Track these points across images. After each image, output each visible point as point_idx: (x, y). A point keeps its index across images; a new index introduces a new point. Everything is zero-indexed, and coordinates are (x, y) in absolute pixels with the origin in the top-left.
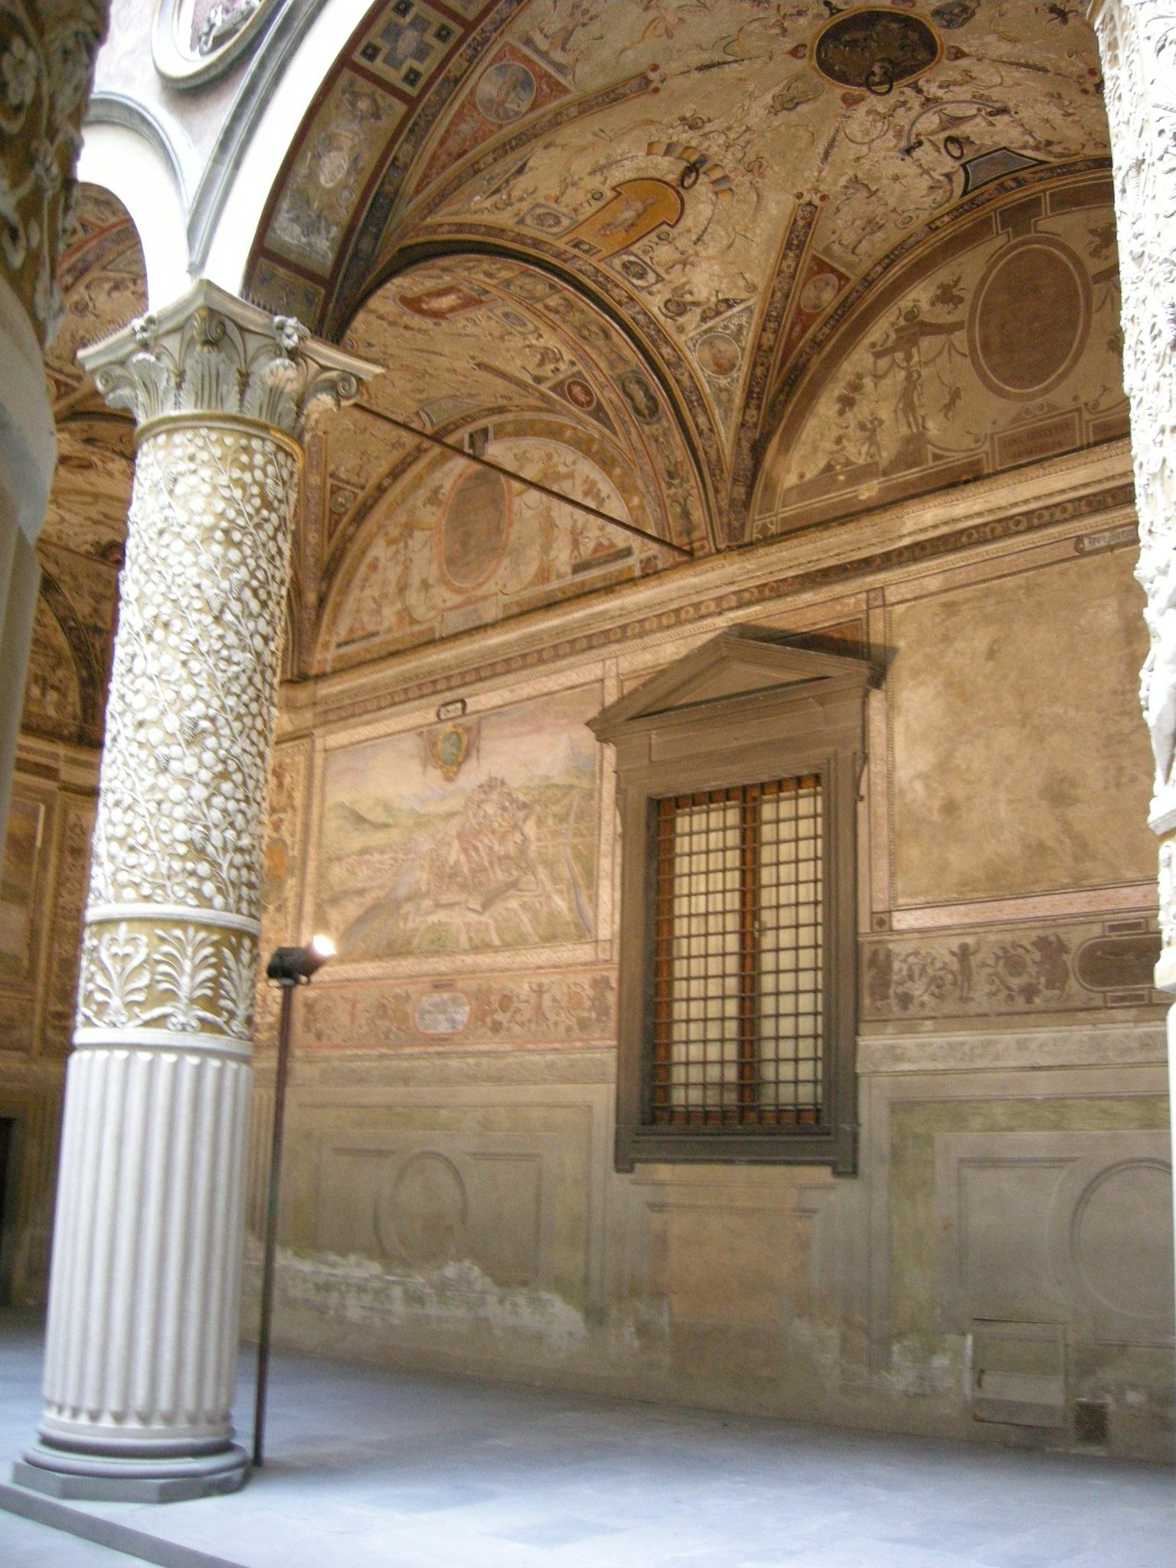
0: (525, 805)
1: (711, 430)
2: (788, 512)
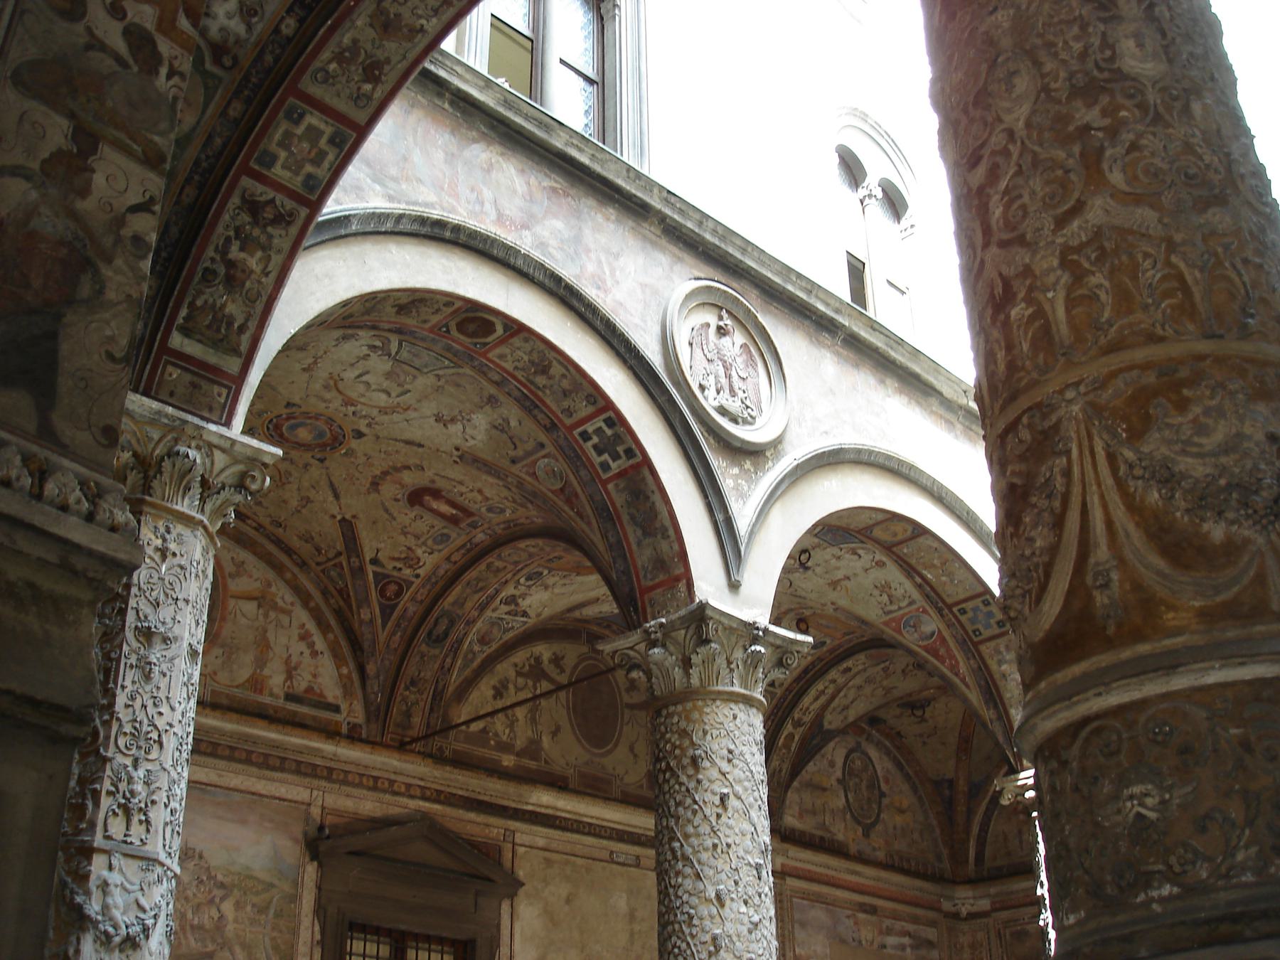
2: (460, 746)
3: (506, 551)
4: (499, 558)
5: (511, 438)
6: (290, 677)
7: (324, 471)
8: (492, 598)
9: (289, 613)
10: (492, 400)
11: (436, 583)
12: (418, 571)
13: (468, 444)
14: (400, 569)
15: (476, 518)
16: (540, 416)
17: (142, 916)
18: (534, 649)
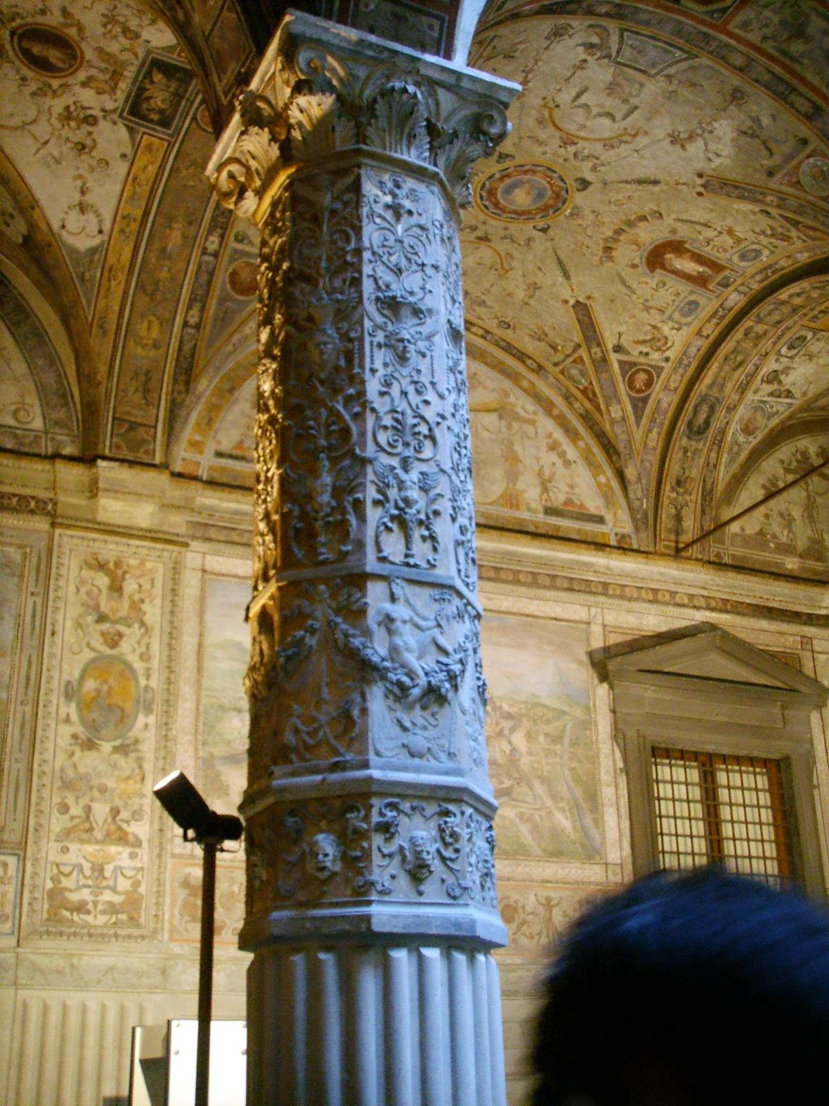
0: (509, 716)
1: (715, 466)
2: (739, 551)
3: (765, 307)
4: (760, 320)
5: (764, 143)
6: (545, 490)
7: (549, 244)
8: (752, 376)
9: (533, 423)
10: (737, 96)
11: (689, 365)
12: (668, 354)
13: (713, 165)
14: (647, 354)
15: (727, 273)
16: (799, 102)
17: (444, 660)
18: (798, 444)
